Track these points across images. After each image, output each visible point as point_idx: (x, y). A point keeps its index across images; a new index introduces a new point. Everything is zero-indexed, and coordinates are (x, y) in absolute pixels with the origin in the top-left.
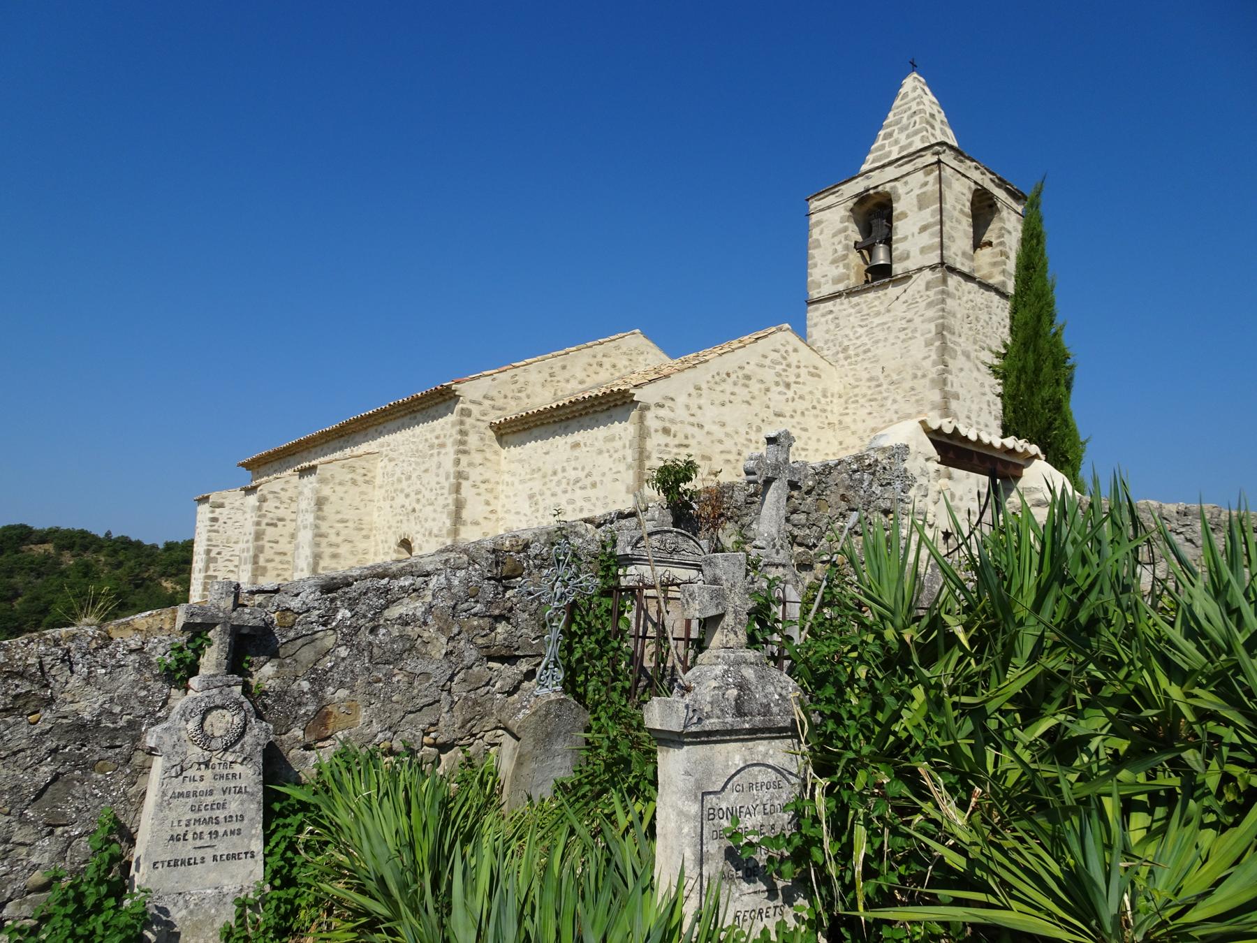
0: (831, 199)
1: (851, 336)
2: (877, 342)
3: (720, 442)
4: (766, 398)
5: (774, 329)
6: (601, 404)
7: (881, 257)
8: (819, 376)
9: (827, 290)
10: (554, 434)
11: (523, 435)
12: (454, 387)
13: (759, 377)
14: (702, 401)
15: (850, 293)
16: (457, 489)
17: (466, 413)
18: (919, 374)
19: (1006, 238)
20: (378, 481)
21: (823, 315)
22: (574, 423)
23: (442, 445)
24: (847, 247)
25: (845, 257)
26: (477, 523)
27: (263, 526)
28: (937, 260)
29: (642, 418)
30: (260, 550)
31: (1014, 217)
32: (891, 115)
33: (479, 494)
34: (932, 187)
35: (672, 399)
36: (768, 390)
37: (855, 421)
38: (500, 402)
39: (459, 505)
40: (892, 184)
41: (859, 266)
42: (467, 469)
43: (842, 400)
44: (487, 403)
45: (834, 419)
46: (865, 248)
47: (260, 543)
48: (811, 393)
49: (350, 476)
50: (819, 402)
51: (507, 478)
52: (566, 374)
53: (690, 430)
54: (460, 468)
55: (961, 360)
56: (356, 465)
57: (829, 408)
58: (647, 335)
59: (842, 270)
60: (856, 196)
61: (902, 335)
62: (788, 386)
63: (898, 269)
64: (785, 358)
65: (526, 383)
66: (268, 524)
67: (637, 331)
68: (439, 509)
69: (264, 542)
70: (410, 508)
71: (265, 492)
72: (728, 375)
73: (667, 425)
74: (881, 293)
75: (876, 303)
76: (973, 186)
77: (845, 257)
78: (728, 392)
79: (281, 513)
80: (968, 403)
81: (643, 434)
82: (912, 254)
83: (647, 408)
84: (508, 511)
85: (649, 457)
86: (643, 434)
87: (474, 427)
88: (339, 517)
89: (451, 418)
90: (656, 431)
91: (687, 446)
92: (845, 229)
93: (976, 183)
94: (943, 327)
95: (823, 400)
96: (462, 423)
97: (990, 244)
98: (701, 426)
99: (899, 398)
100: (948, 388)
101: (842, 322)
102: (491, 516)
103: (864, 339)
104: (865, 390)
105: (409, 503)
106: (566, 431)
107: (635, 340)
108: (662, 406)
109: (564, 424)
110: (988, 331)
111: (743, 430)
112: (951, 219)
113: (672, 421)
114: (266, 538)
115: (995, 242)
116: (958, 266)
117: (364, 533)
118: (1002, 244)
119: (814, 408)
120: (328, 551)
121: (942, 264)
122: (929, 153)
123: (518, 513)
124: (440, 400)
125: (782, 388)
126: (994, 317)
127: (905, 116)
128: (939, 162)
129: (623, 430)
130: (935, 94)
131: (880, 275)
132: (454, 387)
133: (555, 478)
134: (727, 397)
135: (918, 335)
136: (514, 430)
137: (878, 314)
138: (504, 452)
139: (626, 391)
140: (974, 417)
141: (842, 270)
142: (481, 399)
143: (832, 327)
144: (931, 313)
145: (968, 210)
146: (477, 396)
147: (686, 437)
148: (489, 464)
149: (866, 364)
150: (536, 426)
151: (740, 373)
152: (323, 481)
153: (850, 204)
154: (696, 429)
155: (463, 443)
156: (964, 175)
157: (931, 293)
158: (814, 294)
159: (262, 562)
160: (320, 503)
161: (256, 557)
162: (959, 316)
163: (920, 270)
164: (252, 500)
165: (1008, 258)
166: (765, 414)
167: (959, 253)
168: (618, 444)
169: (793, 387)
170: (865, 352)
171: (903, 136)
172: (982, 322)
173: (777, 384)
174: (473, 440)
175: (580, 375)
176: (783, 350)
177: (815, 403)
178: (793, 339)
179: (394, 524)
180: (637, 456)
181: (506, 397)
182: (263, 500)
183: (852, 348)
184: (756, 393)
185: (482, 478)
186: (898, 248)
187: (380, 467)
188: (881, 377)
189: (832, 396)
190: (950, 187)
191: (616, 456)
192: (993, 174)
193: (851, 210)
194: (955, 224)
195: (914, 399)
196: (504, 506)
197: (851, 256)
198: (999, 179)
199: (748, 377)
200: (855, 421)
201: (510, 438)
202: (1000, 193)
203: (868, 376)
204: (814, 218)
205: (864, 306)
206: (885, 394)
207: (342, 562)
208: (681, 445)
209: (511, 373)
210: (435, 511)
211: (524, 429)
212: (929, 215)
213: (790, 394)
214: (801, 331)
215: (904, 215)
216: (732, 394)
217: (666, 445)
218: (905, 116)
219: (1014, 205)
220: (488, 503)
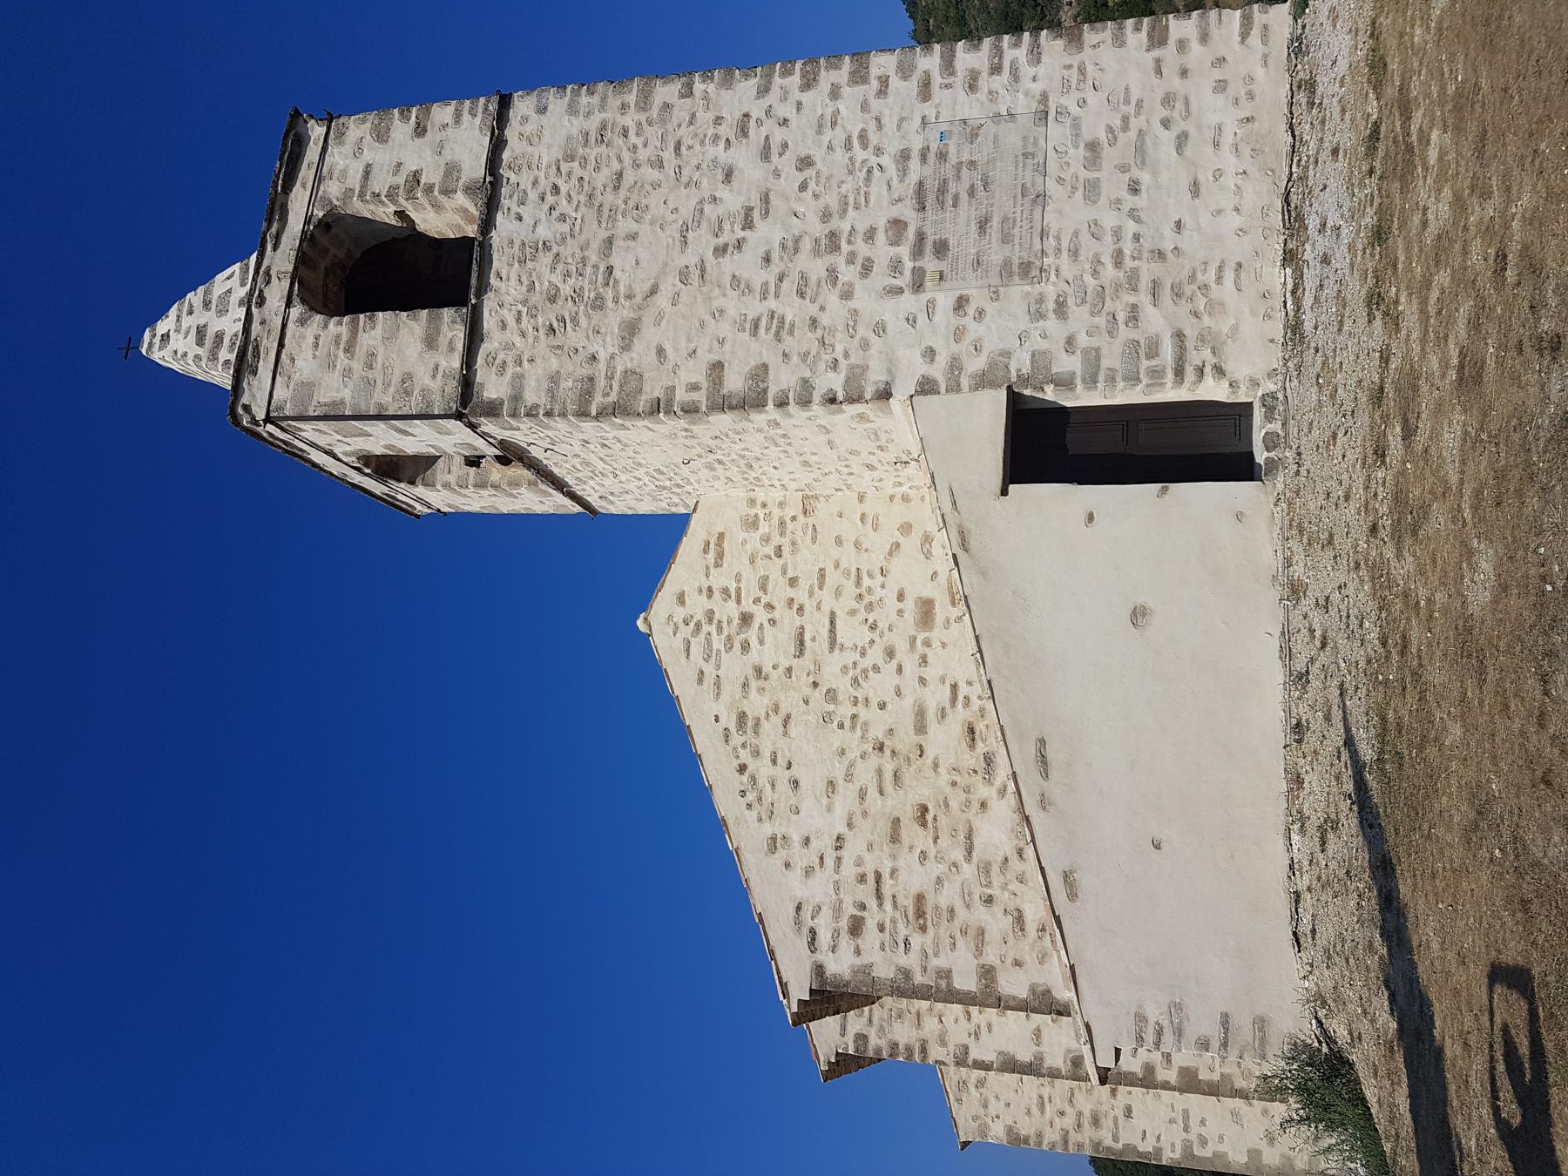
0: (400, 497)
3: (862, 795)
4: (774, 675)
14: (796, 838)
19: (380, 183)
31: (338, 157)
33: (990, 1026)
35: (799, 908)
36: (758, 671)
39: (1011, 1066)
42: (951, 1048)
48: (752, 562)
49: (972, 1089)
50: (766, 539)
55: (641, 355)
56: (955, 1078)
64: (698, 626)
73: (844, 924)
76: (296, 311)
80: (725, 329)
83: (819, 970)
85: (907, 974)
87: (882, 1028)
88: (1035, 1110)
90: (858, 952)
91: (878, 877)
92: (447, 486)
93: (289, 304)
95: (764, 528)
97: (401, 214)
100: (701, 397)
108: (813, 932)
110: (570, 250)
111: (837, 738)
112: (370, 383)
113: (837, 911)
115: (393, 208)
118: (392, 195)
119: (779, 552)
121: (459, 416)
126: (543, 232)
130: (162, 313)
134: (783, 776)
135: (610, 436)
140: (755, 308)
145: (339, 327)
151: (737, 739)
154: (844, 853)
156: (281, 345)
162: (554, 363)
165: (416, 177)
166: (802, 681)
167: (431, 358)
169: (747, 605)
170: (662, 473)
172: (556, 279)
173: (746, 647)
177: (770, 550)
184: (766, 701)
189: (752, 502)
190: (307, 388)
193: (412, 483)
194: (376, 374)
198: (270, 222)
199: (742, 717)
202: (298, 204)
207: (1104, 1108)
208: (879, 896)
216: (774, 762)
217: (882, 929)
219: (312, 153)
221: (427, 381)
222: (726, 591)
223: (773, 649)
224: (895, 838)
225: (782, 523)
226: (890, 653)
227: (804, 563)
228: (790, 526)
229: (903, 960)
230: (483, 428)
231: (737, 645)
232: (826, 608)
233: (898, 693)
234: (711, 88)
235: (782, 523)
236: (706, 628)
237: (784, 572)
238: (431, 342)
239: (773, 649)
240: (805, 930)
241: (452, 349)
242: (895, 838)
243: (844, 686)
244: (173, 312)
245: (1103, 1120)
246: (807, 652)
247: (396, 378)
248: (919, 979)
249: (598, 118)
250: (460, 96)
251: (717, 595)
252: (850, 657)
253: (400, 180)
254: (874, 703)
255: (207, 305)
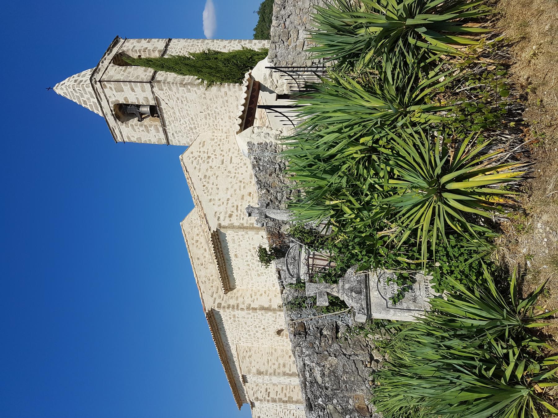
0: (117, 131)
1: (185, 126)
2: (188, 114)
3: (235, 190)
5: (182, 163)
6: (217, 245)
7: (147, 110)
8: (204, 142)
9: (162, 136)
10: (230, 265)
11: (230, 279)
12: (207, 312)
13: (205, 171)
14: (217, 199)
15: (164, 125)
16: (255, 309)
17: (219, 305)
18: (204, 96)
19: (137, 48)
20: (250, 345)
21: (175, 138)
22: (225, 257)
23: (234, 316)
24: (141, 125)
25: (146, 126)
26: (270, 300)
27: (270, 398)
28: (149, 84)
29: (224, 227)
30: (280, 400)
31: (126, 44)
32: (74, 101)
34: (112, 85)
36: (211, 167)
37: (225, 126)
38: (214, 289)
39: (262, 308)
40: (110, 103)
41: (150, 120)
42: (246, 305)
43: (215, 131)
44: (215, 296)
45: (224, 135)
46: (141, 117)
47: (277, 400)
48: (212, 146)
49: (247, 358)
50: (216, 142)
51: (249, 286)
52: (201, 257)
53: (230, 205)
54: (245, 308)
57: (219, 138)
58: (183, 219)
59: (152, 128)
60: (115, 120)
61: (185, 103)
62: (209, 157)
63: (152, 103)
64: (196, 158)
65: (206, 277)
66: (269, 397)
67: (181, 223)
68: (264, 317)
69: (277, 398)
70: (263, 330)
71: (253, 398)
72: (204, 186)
73: (227, 215)
74: (164, 111)
75: (169, 113)
77: (146, 126)
78: (212, 186)
79: (263, 390)
81: (232, 227)
82: (145, 96)
83: (220, 225)
84: (265, 286)
85: (242, 224)
86: (232, 227)
88: (266, 364)
89: (221, 312)
90: (230, 221)
91: (237, 206)
92: (132, 125)
93: (110, 63)
94: (181, 84)
95: (216, 140)
96: (224, 307)
98: (228, 199)
99: (215, 106)
101: (178, 130)
102: (267, 293)
103: (186, 120)
104: (211, 121)
105: (261, 331)
106: (229, 260)
107: (185, 225)
108: (219, 217)
109: (226, 261)
113: (226, 213)
114: (275, 397)
116: (151, 74)
117: (273, 352)
118: (140, 51)
119: (219, 145)
120: (282, 369)
121: (150, 82)
122: (95, 86)
123: (266, 281)
124: (213, 318)
125: (210, 160)
127: (75, 94)
128: (100, 81)
129: (230, 236)
131: (155, 111)
132: (207, 312)
133: (251, 265)
134: (215, 187)
135: (185, 96)
136: (228, 284)
137: (174, 113)
138: (238, 287)
139: (212, 235)
141: (152, 128)
142: (213, 298)
143: (180, 134)
144: (174, 89)
146: (212, 300)
147: (233, 206)
148: (243, 295)
149: (199, 120)
150: (226, 273)
151: (203, 180)
152: (249, 372)
153: (119, 123)
155: (233, 307)
156: (106, 69)
157: (164, 88)
158: (164, 141)
159: (286, 399)
160: (260, 373)
161: (283, 402)
163: (153, 92)
164: (257, 404)
165: (147, 48)
168: (236, 238)
170: (193, 120)
171: (85, 96)
173: (208, 162)
174: (232, 302)
175: (202, 251)
176: (192, 159)
178: (187, 154)
179: (270, 337)
180: (242, 230)
181: (212, 287)
182: (257, 399)
183: (190, 126)
184: (212, 173)
185: (250, 298)
186: (142, 102)
187: (243, 345)
188: (205, 113)
189: (213, 136)
190: (112, 77)
191: (241, 239)
192: (105, 54)
193: (122, 122)
195: (215, 99)
196: (263, 287)
197: (146, 124)
198: (108, 51)
199: (205, 176)
200: (225, 126)
201: (231, 285)
202: (115, 51)
203: (204, 119)
204: (126, 140)
205: (170, 119)
206: (213, 112)
209: (201, 284)
210: (264, 319)
211: (228, 278)
212: (126, 87)
213: (213, 156)
214: (183, 149)
215: (126, 99)
217: (237, 216)
218: (75, 94)
219: (120, 43)
220: (261, 295)
221: (143, 77)
222: (204, 152)
223: (215, 163)
224: (242, 198)
225: (220, 140)
226: (245, 164)
227: (226, 147)
228: (222, 140)
229: (242, 222)
230: (154, 89)
231: (206, 162)
232: (230, 156)
233: (246, 171)
234: (218, 42)
235: (220, 140)
236: (198, 159)
237: (220, 148)
238: (145, 71)
239: (215, 163)
240: (217, 217)
241: (150, 72)
242: (242, 198)
243: (233, 171)
244: (67, 79)
245: (286, 365)
246: (224, 164)
247: (135, 76)
248: (245, 225)
249: (192, 43)
250: (159, 38)
251: (202, 152)
252: (235, 165)
253: (143, 48)
254: (240, 173)
255: (78, 76)
